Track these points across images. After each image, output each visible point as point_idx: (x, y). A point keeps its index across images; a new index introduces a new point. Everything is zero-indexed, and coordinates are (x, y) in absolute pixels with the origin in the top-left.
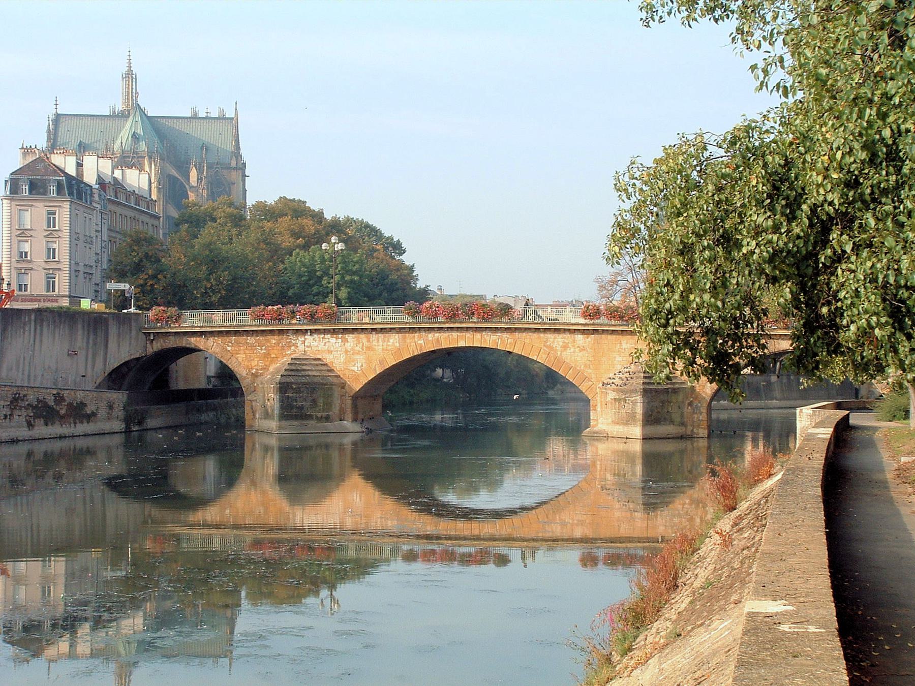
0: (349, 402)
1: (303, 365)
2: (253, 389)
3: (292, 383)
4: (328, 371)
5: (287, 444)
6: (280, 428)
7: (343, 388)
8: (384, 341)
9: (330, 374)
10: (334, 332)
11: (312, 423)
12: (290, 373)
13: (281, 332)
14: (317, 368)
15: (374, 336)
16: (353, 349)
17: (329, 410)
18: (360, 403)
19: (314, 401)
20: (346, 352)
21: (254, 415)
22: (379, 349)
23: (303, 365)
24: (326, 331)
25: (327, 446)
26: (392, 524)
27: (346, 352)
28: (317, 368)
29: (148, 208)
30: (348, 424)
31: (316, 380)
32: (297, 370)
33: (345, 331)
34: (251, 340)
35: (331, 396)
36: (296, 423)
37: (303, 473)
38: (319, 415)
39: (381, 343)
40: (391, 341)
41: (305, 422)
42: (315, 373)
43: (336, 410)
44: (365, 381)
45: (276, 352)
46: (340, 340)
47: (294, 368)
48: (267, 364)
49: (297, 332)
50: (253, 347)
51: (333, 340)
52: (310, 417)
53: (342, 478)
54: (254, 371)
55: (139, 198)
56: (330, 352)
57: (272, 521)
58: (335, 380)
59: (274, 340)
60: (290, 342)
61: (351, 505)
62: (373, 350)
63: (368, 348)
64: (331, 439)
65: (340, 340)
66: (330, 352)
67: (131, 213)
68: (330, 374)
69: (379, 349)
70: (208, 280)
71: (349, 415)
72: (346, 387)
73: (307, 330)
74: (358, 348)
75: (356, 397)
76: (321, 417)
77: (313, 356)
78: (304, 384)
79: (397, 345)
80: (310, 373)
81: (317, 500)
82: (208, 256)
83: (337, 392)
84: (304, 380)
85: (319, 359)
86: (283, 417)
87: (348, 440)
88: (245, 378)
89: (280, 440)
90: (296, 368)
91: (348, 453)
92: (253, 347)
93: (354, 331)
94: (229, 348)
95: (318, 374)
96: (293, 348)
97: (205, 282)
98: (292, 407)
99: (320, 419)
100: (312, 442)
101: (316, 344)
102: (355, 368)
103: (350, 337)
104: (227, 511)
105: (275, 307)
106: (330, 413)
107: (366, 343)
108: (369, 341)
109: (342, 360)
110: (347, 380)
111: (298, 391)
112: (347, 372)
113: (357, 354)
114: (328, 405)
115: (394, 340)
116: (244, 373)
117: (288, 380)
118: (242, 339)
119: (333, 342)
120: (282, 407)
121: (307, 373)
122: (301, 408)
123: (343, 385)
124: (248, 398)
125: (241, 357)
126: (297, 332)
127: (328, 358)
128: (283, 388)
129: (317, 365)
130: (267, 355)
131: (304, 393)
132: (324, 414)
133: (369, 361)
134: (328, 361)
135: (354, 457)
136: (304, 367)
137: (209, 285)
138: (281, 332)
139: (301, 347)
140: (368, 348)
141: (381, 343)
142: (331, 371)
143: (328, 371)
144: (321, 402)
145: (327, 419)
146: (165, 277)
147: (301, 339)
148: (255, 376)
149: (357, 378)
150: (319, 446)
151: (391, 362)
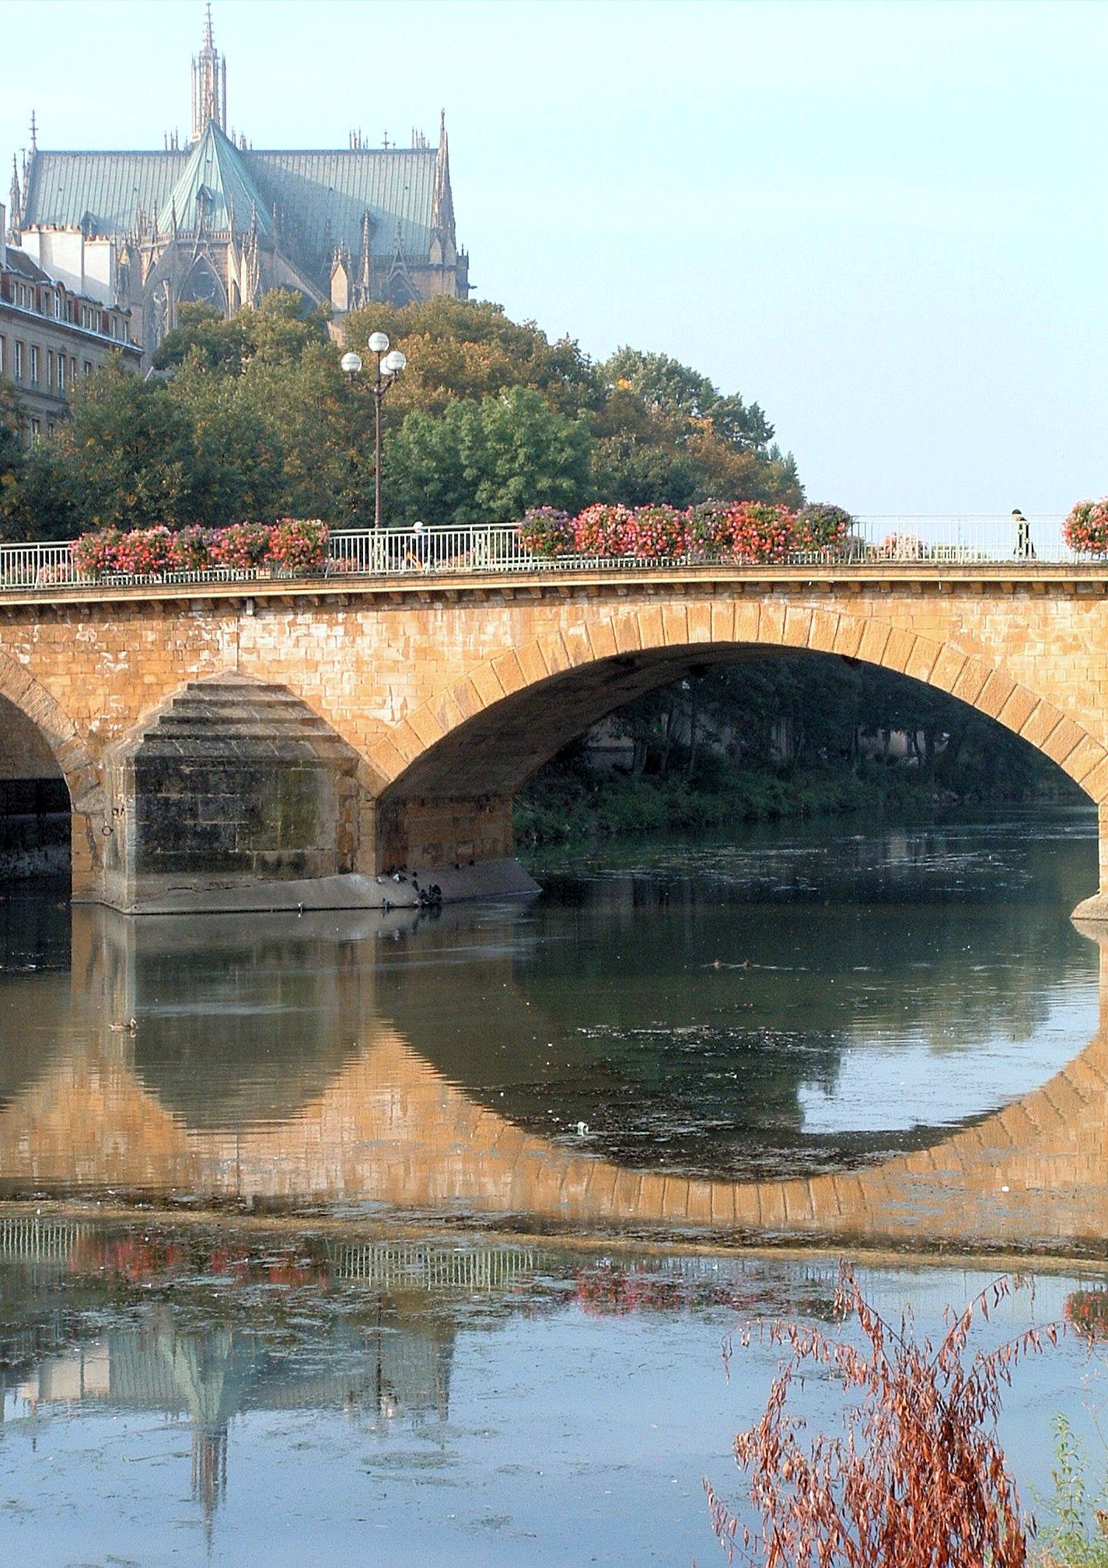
0: (368, 816)
1: (224, 704)
2: (92, 780)
3: (179, 760)
4: (306, 722)
5: (156, 944)
6: (141, 896)
7: (349, 773)
8: (468, 631)
9: (308, 731)
10: (323, 604)
11: (245, 880)
12: (174, 730)
13: (170, 607)
14: (272, 714)
15: (438, 616)
16: (377, 656)
17: (305, 839)
18: (413, 819)
19: (253, 813)
20: (359, 664)
21: (97, 858)
22: (454, 654)
23: (224, 704)
24: (297, 603)
25: (299, 950)
26: (501, 1191)
27: (359, 664)
28: (272, 714)
29: (39, 310)
30: (365, 884)
31: (260, 750)
32: (203, 721)
33: (354, 601)
34: (86, 632)
35: (310, 798)
36: (193, 880)
37: (221, 1037)
38: (270, 856)
39: (459, 638)
40: (490, 629)
41: (225, 879)
42: (259, 730)
43: (326, 839)
44: (411, 752)
45: (156, 667)
46: (339, 630)
47: (191, 713)
48: (134, 703)
49: (216, 606)
50: (91, 653)
51: (320, 630)
52: (241, 863)
53: (349, 1046)
54: (94, 726)
55: (76, 305)
56: (312, 665)
57: (150, 1175)
58: (325, 752)
59: (150, 631)
60: (198, 638)
61: (379, 1130)
62: (439, 658)
63: (424, 653)
64: (306, 928)
65: (339, 630)
66: (312, 665)
67: (57, 342)
68: (308, 731)
69: (454, 654)
70: (130, 487)
71: (368, 856)
72: (360, 772)
73: (243, 601)
74: (393, 654)
75: (393, 804)
76: (279, 863)
77: (264, 679)
78: (217, 762)
79: (508, 641)
80: (243, 730)
81: (280, 1114)
82: (129, 421)
83: (329, 788)
84: (220, 750)
85: (280, 688)
86: (148, 863)
87: (364, 931)
88: (70, 748)
89: (139, 930)
90: (197, 715)
91: (368, 967)
92: (91, 653)
93: (379, 600)
94: (25, 659)
95: (269, 731)
96: (205, 655)
97: (121, 492)
98: (180, 833)
99: (273, 869)
100: (246, 938)
101: (270, 641)
102: (385, 714)
103: (369, 620)
104: (24, 1146)
105: (150, 534)
106: (308, 851)
107: (415, 638)
108: (424, 629)
109: (347, 688)
110: (361, 749)
111: (198, 783)
112: (360, 725)
113: (388, 673)
114: (300, 826)
115: (499, 625)
116: (68, 733)
117: (167, 751)
118: (60, 630)
119: (318, 634)
120: (147, 834)
121: (233, 730)
122: (213, 834)
123: (350, 767)
124: (79, 805)
125: (58, 684)
126: (216, 606)
127: (305, 685)
128: (150, 774)
129: (270, 705)
130: (131, 678)
131: (223, 789)
132: (288, 853)
133: (425, 690)
134: (298, 695)
135: (389, 979)
136: (226, 712)
137: (131, 501)
138: (170, 607)
139: (228, 653)
140: (424, 653)
141: (459, 638)
142: (314, 722)
143: (306, 722)
144: (275, 816)
145: (299, 867)
146: (19, 480)
147: (228, 626)
148: (99, 739)
149: (389, 742)
150: (274, 949)
151: (491, 693)
